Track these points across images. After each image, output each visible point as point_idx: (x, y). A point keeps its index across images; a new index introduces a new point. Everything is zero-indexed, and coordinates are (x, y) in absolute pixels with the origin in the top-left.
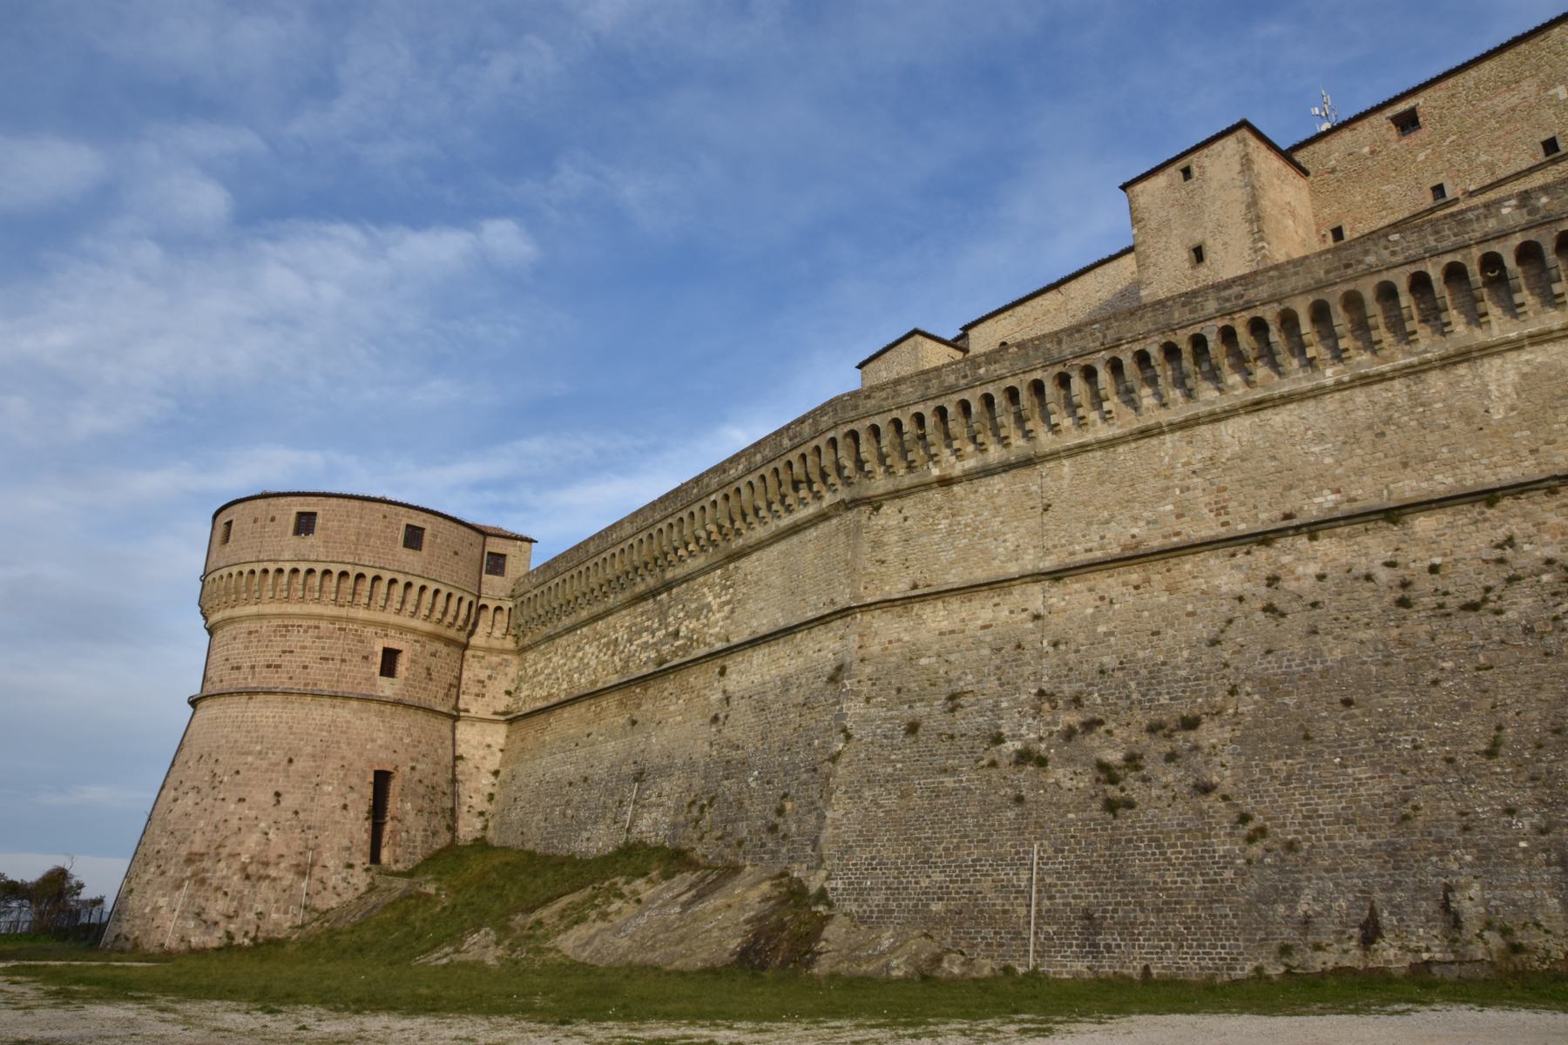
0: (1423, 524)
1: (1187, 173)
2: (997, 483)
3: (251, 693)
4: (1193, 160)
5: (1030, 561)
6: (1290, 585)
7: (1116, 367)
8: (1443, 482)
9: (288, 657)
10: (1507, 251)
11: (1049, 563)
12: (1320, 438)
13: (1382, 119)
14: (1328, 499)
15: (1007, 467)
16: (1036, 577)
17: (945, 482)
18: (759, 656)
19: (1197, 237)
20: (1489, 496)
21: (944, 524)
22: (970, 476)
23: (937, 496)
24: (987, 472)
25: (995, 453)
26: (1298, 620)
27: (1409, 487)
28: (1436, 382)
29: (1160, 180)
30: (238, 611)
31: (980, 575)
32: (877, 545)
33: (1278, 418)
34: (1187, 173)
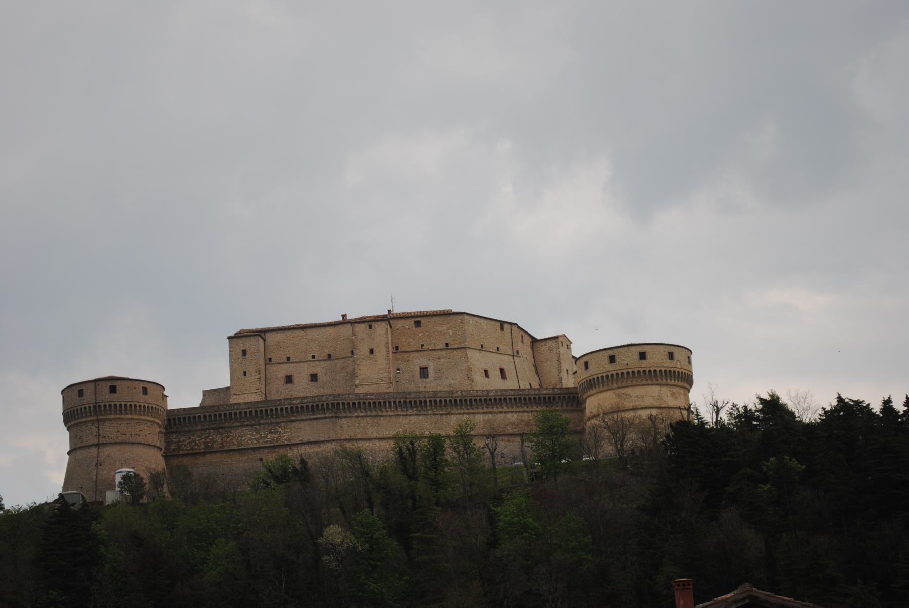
1: (370, 327)
2: (368, 419)
3: (133, 443)
4: (373, 324)
5: (375, 435)
7: (395, 402)
10: (458, 399)
11: (379, 436)
13: (412, 321)
17: (357, 417)
18: (306, 446)
19: (372, 347)
22: (362, 416)
23: (354, 419)
24: (367, 416)
25: (368, 413)
28: (444, 417)
29: (363, 326)
30: (122, 416)
31: (365, 436)
32: (341, 427)
33: (421, 417)
34: (370, 327)
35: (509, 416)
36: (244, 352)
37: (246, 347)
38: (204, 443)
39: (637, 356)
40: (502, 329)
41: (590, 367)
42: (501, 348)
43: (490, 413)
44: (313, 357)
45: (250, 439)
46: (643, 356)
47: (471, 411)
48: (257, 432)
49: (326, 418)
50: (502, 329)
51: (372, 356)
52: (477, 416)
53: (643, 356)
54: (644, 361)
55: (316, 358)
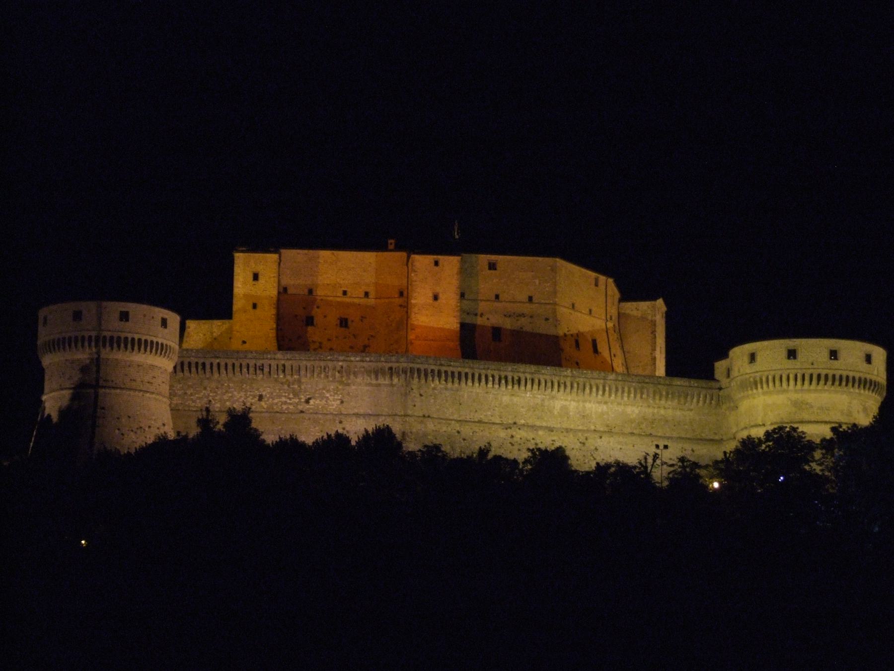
0: (541, 433)
2: (448, 393)
5: (456, 417)
6: (515, 439)
8: (544, 424)
9: (154, 380)
12: (523, 407)
14: (523, 422)
15: (452, 390)
16: (458, 421)
17: (434, 389)
20: (551, 430)
21: (432, 401)
24: (446, 389)
26: (516, 447)
27: (538, 423)
34: (436, 263)
35: (629, 410)
36: (256, 277)
37: (260, 269)
38: (220, 401)
39: (826, 354)
40: (596, 285)
41: (758, 358)
42: (594, 309)
43: (606, 403)
44: (345, 293)
45: (285, 403)
46: (834, 354)
47: (581, 397)
48: (296, 395)
49: (392, 385)
50: (596, 285)
51: (436, 303)
52: (588, 405)
53: (834, 354)
54: (835, 362)
55: (349, 294)
